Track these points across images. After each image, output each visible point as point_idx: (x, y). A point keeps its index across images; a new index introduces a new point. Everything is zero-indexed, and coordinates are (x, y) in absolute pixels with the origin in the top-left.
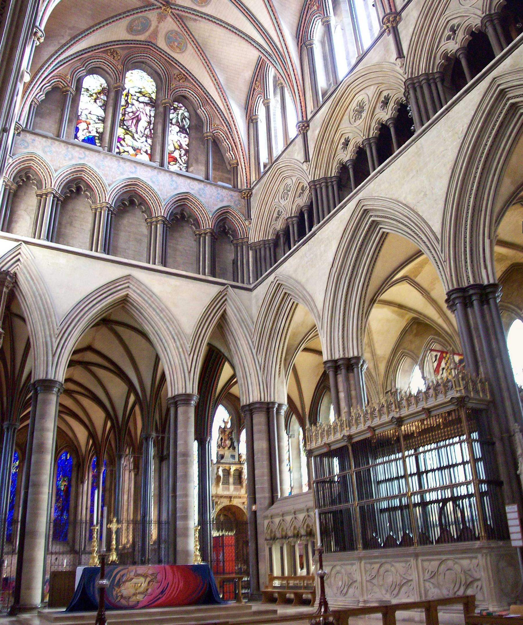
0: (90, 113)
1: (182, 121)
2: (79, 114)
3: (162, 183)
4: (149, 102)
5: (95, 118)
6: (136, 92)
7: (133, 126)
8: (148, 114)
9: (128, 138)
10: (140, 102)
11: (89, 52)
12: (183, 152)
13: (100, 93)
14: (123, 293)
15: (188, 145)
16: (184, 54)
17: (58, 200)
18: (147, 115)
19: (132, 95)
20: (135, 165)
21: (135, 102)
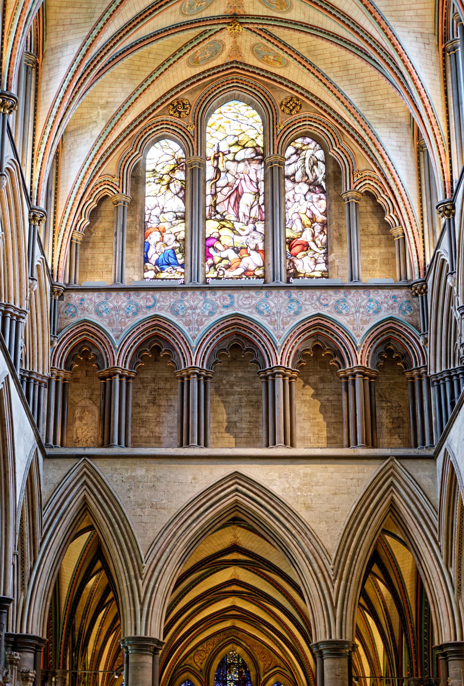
0: (162, 212)
1: (312, 170)
2: (147, 220)
3: (274, 310)
4: (254, 155)
5: (169, 216)
6: (230, 146)
7: (230, 209)
8: (254, 179)
9: (225, 232)
10: (239, 162)
11: (140, 123)
12: (318, 228)
13: (173, 170)
14: (229, 501)
15: (325, 213)
16: (288, 68)
17: (128, 378)
18: (251, 180)
19: (224, 155)
20: (229, 292)
21: (231, 166)
